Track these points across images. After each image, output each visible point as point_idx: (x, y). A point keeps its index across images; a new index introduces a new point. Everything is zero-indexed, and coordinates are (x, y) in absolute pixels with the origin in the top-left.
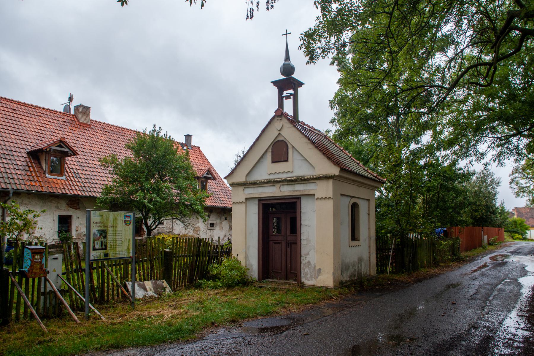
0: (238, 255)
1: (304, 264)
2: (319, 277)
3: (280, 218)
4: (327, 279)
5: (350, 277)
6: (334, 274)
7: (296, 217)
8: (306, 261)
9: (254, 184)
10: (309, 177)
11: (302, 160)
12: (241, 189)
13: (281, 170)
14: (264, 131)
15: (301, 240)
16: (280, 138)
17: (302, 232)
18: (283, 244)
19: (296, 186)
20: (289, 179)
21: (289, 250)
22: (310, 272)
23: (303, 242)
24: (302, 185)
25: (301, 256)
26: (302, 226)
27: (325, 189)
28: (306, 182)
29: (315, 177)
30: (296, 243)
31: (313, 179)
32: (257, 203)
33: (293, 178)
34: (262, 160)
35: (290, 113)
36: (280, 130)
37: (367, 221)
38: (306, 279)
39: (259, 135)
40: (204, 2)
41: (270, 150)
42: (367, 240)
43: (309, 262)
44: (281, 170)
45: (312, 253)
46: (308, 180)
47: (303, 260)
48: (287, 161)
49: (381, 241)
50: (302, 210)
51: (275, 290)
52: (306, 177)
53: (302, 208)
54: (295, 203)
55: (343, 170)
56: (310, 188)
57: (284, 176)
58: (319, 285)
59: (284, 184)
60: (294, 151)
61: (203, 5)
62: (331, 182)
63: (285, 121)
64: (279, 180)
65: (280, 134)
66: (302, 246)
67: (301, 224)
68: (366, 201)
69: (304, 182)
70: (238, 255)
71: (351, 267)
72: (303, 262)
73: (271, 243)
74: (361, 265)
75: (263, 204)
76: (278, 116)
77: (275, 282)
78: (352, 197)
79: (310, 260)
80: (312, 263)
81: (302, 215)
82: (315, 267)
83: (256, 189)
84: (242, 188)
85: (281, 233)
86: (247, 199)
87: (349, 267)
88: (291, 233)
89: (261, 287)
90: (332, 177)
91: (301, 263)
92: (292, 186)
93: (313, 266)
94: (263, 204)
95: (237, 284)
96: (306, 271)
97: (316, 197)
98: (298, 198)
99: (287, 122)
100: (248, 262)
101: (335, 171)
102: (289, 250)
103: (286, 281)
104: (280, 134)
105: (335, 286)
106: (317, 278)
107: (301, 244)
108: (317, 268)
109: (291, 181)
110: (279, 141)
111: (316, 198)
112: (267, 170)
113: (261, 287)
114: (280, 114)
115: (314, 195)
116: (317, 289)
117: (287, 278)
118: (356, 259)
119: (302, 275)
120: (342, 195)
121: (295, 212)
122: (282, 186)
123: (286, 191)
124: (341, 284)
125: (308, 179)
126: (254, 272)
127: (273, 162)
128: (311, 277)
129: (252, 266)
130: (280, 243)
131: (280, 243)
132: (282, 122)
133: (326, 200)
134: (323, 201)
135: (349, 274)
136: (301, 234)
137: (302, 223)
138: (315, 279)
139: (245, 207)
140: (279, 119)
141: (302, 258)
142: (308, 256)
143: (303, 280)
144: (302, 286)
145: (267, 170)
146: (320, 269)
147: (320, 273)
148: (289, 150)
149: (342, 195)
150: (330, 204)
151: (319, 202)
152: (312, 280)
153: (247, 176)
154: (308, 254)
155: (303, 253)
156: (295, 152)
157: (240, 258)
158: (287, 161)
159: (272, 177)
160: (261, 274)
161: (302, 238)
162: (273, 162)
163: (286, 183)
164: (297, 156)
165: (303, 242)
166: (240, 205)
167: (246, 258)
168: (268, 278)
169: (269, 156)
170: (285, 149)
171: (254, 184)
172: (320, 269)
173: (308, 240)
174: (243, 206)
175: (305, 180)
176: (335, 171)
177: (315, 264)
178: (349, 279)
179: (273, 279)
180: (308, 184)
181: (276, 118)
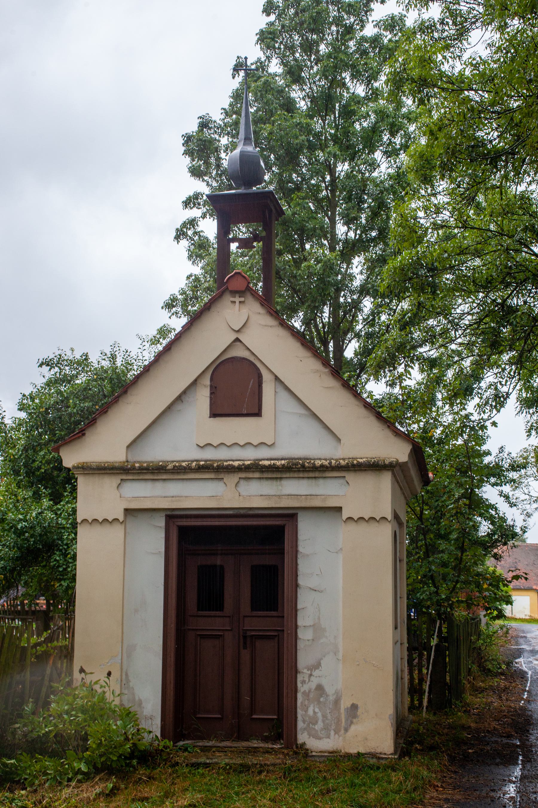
0: (109, 674)
1: (306, 694)
2: (353, 728)
4: (374, 732)
8: (313, 685)
9: (157, 471)
10: (326, 463)
11: (301, 415)
12: (109, 483)
13: (238, 439)
15: (296, 627)
16: (239, 352)
17: (299, 606)
19: (284, 482)
20: (267, 463)
21: (246, 655)
22: (324, 716)
23: (304, 635)
24: (305, 482)
25: (296, 672)
28: (317, 474)
29: (343, 463)
31: (339, 468)
33: (278, 463)
34: (179, 407)
36: (238, 331)
38: (310, 735)
41: (207, 381)
43: (320, 688)
44: (238, 439)
45: (327, 663)
46: (323, 469)
47: (303, 682)
48: (258, 414)
50: (300, 549)
52: (318, 463)
56: (328, 491)
57: (249, 455)
58: (353, 751)
59: (251, 475)
60: (280, 389)
64: (236, 464)
65: (237, 340)
66: (301, 645)
67: (297, 586)
69: (311, 475)
70: (109, 674)
72: (302, 688)
79: (324, 682)
80: (330, 690)
81: (300, 561)
82: (337, 702)
83: (159, 485)
84: (114, 481)
86: (127, 511)
88: (253, 609)
92: (274, 483)
93: (332, 698)
96: (310, 712)
97: (345, 516)
102: (246, 655)
103: (245, 744)
104: (237, 340)
106: (346, 730)
108: (345, 704)
109: (272, 469)
110: (233, 359)
111: (344, 517)
113: (196, 766)
119: (300, 725)
121: (281, 552)
122: (242, 482)
123: (256, 495)
125: (322, 466)
127: (214, 414)
128: (326, 728)
129: (140, 703)
131: (217, 637)
133: (374, 525)
134: (363, 526)
137: (301, 581)
138: (337, 732)
140: (237, 299)
141: (300, 678)
142: (316, 673)
143: (302, 737)
144: (302, 752)
146: (354, 707)
147: (355, 716)
148: (264, 385)
151: (352, 526)
152: (328, 737)
153: (128, 447)
154: (318, 666)
155: (304, 660)
156: (283, 395)
158: (258, 414)
159: (209, 455)
161: (300, 623)
162: (214, 414)
163: (257, 475)
164: (286, 404)
165: (300, 634)
166: (106, 530)
169: (202, 398)
171: (157, 471)
173: (317, 628)
174: (118, 531)
175: (315, 469)
180: (321, 481)
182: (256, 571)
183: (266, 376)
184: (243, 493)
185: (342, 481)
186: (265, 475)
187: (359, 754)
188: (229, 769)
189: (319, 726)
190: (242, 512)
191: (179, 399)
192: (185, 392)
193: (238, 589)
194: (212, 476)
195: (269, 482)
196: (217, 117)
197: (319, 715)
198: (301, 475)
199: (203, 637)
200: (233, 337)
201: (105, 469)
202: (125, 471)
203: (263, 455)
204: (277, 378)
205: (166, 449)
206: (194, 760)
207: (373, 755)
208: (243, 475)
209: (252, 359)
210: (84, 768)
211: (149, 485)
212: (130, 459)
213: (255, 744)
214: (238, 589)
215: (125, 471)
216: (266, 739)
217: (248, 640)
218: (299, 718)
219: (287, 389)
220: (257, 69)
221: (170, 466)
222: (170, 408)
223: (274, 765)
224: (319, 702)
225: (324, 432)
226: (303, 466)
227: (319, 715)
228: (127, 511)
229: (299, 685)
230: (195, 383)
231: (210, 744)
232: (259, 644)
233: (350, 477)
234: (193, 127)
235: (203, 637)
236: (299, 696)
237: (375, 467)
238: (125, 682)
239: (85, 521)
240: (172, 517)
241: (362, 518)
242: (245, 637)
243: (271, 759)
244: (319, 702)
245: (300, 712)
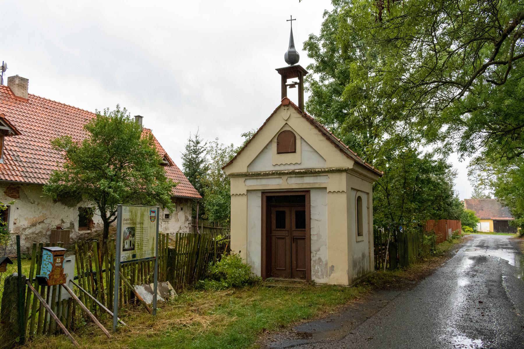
0: (240, 252)
1: (315, 261)
2: (332, 274)
3: (287, 212)
4: (341, 277)
5: (357, 274)
6: (348, 271)
7: (305, 211)
9: (258, 175)
10: (320, 170)
11: (311, 152)
12: (242, 180)
13: (287, 162)
14: (268, 120)
15: (310, 235)
17: (311, 227)
18: (288, 240)
19: (305, 178)
20: (297, 171)
21: (294, 245)
23: (313, 238)
25: (311, 253)
27: (339, 183)
28: (317, 175)
29: (326, 170)
31: (325, 172)
33: (302, 171)
34: (266, 150)
36: (286, 120)
38: (316, 277)
41: (276, 140)
43: (320, 259)
44: (287, 162)
45: (323, 249)
46: (319, 172)
47: (313, 256)
48: (295, 152)
49: (377, 236)
50: (311, 204)
51: (287, 289)
52: (317, 170)
53: (311, 202)
54: (304, 196)
55: (357, 163)
56: (321, 181)
57: (291, 168)
58: (333, 284)
59: (292, 176)
60: (303, 142)
62: (344, 175)
63: (292, 111)
64: (286, 172)
65: (286, 124)
66: (312, 242)
67: (310, 219)
69: (315, 175)
70: (240, 252)
72: (313, 259)
73: (274, 238)
75: (267, 197)
76: (285, 106)
78: (358, 190)
80: (324, 260)
82: (326, 264)
83: (259, 180)
84: (243, 179)
85: (284, 228)
86: (248, 191)
88: (297, 228)
89: (270, 287)
90: (346, 171)
91: (311, 260)
94: (267, 197)
95: (243, 283)
96: (316, 268)
97: (328, 190)
98: (307, 191)
100: (249, 259)
101: (349, 164)
102: (294, 245)
103: (292, 280)
105: (350, 285)
106: (330, 276)
108: (330, 265)
110: (285, 131)
111: (328, 191)
112: (271, 161)
113: (270, 287)
114: (286, 103)
115: (326, 188)
116: (335, 288)
117: (292, 277)
118: (361, 256)
119: (312, 273)
120: (352, 189)
121: (304, 206)
124: (355, 283)
125: (318, 171)
127: (278, 153)
128: (322, 275)
129: (254, 263)
130: (283, 238)
131: (283, 238)
132: (289, 113)
134: (335, 195)
136: (310, 229)
137: (312, 217)
139: (246, 199)
140: (286, 108)
141: (312, 255)
142: (318, 253)
143: (313, 278)
144: (313, 284)
145: (271, 161)
146: (333, 266)
147: (333, 270)
148: (297, 141)
149: (352, 189)
150: (343, 198)
151: (331, 195)
152: (323, 278)
153: (248, 166)
154: (319, 250)
155: (313, 248)
156: (304, 143)
157: (242, 256)
158: (295, 152)
159: (277, 168)
161: (312, 233)
162: (278, 153)
163: (294, 176)
164: (305, 147)
165: (312, 238)
166: (241, 197)
167: (248, 255)
168: (271, 276)
169: (274, 147)
170: (292, 140)
171: (258, 175)
172: (333, 266)
173: (318, 235)
174: (244, 199)
175: (316, 172)
176: (349, 164)
177: (327, 262)
179: (278, 277)
180: (319, 177)
181: (283, 108)
182: (297, 213)
183: (298, 137)
184: (289, 183)
185: (326, 177)
186: (297, 176)
187: (335, 285)
188: (281, 289)
189: (320, 273)
190: (289, 190)
191: (266, 147)
192: (268, 145)
193: (290, 220)
194: (278, 176)
195: (299, 178)
196: (318, 34)
197: (320, 269)
198: (311, 175)
199: (278, 238)
200: (285, 122)
201: (239, 175)
202: (246, 176)
203: (297, 168)
204: (301, 138)
205: (260, 167)
206: (270, 285)
207: (340, 286)
208: (289, 176)
209: (292, 131)
210: (226, 285)
211: (255, 180)
212: (249, 171)
213: (281, 279)
214: (290, 220)
215: (246, 176)
216: (302, 278)
217: (295, 240)
218: (312, 270)
219: (305, 141)
220: (334, 13)
221: (262, 173)
222: (262, 151)
223: (298, 288)
224: (320, 264)
225: (320, 158)
226: (311, 172)
227: (320, 269)
228: (248, 191)
229: (312, 257)
230: (271, 141)
231: (295, 280)
232: (299, 241)
233: (330, 175)
235: (278, 238)
236: (312, 262)
237: (339, 171)
238: (248, 255)
239: (233, 195)
240: (264, 192)
242: (294, 239)
243: (299, 286)
244: (320, 264)
245: (312, 268)
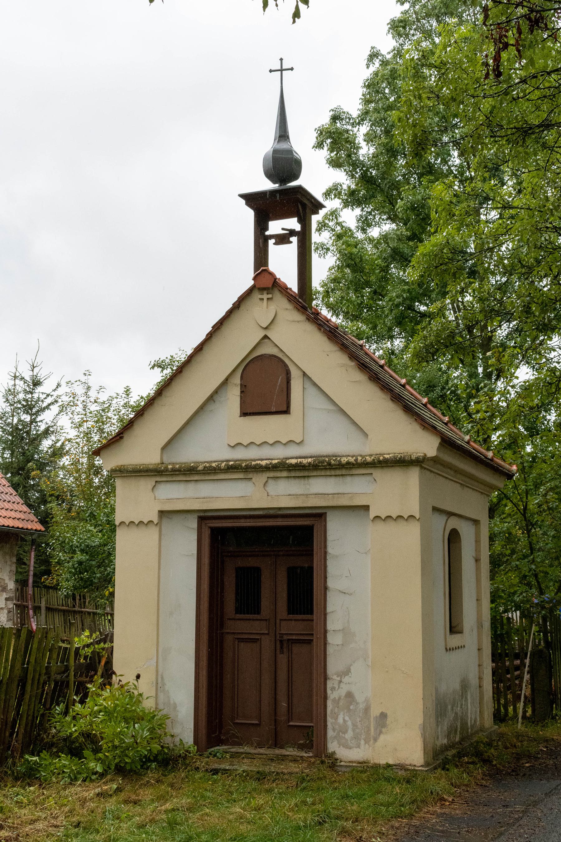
0: (138, 677)
1: (336, 702)
2: (382, 737)
3: (263, 570)
4: (404, 743)
5: (448, 736)
6: (424, 728)
7: (311, 569)
8: (342, 692)
9: (189, 472)
10: (352, 460)
11: (329, 411)
12: (146, 484)
13: (268, 437)
14: (218, 326)
15: (326, 631)
16: (267, 350)
17: (329, 610)
18: (267, 643)
19: (312, 481)
20: (293, 461)
21: (283, 659)
22: (354, 725)
23: (334, 639)
24: (332, 480)
25: (326, 678)
26: (329, 594)
27: (401, 493)
28: (344, 472)
29: (369, 459)
30: (310, 642)
31: (365, 465)
32: (195, 525)
33: (305, 461)
35: (291, 281)
36: (266, 328)
37: (474, 580)
38: (340, 744)
39: (203, 337)
40: (300, 4)
41: (237, 380)
42: (475, 631)
43: (349, 695)
44: (268, 437)
45: (358, 669)
46: (349, 466)
47: (333, 689)
48: (287, 411)
49: (500, 632)
50: (330, 550)
51: (261, 777)
52: (344, 460)
53: (330, 544)
54: (309, 529)
55: (447, 443)
56: (355, 488)
57: (277, 454)
58: (383, 762)
59: (278, 474)
60: (308, 385)
61: (297, 14)
62: (414, 476)
63: (281, 304)
64: (264, 463)
65: (266, 337)
66: (330, 650)
67: (326, 588)
68: (470, 524)
69: (338, 472)
70: (138, 677)
71: (449, 707)
72: (332, 695)
73: (229, 639)
74: (466, 700)
75: (213, 530)
76: (262, 290)
77: (248, 755)
78: (450, 514)
79: (353, 689)
80: (360, 698)
81: (329, 563)
82: (367, 710)
83: (191, 486)
84: (150, 482)
85: (259, 613)
86: (162, 513)
87: (446, 706)
89: (215, 772)
90: (418, 462)
91: (325, 698)
92: (302, 481)
93: (362, 706)
94: (213, 530)
95: (146, 761)
96: (340, 720)
97: (373, 513)
98: (319, 516)
99: (288, 306)
100: (161, 696)
101: (428, 446)
102: (283, 659)
103: (278, 751)
104: (266, 337)
105: (427, 764)
106: (375, 740)
107: (325, 644)
108: (375, 712)
109: (299, 467)
111: (372, 515)
112: (226, 434)
113: (215, 772)
114: (265, 283)
115: (366, 508)
116: (387, 774)
117: (277, 743)
118: (457, 686)
119: (330, 733)
120: (435, 509)
121: (310, 554)
122: (270, 481)
123: (284, 495)
124: (441, 758)
125: (348, 463)
126: (183, 726)
127: (244, 414)
128: (356, 737)
130: (255, 641)
131: (255, 641)
132: (273, 308)
133: (402, 523)
134: (391, 527)
135: (445, 728)
136: (325, 615)
138: (367, 742)
139: (156, 537)
140: (265, 296)
141: (329, 684)
142: (346, 679)
143: (333, 746)
144: (333, 763)
145: (226, 434)
146: (383, 716)
147: (384, 725)
148: (293, 382)
149: (435, 509)
150: (411, 535)
151: (380, 527)
152: (358, 746)
153: (163, 449)
154: (347, 672)
155: (334, 666)
156: (311, 390)
157: (145, 687)
158: (287, 411)
159: (241, 454)
160: (203, 731)
161: (330, 627)
163: (285, 474)
164: (315, 401)
165: (331, 638)
167: (159, 685)
168: (220, 742)
169: (233, 396)
170: (281, 380)
171: (189, 472)
172: (383, 716)
173: (346, 632)
174: (152, 534)
175: (341, 466)
176: (428, 446)
177: (367, 701)
178: (445, 741)
179: (239, 744)
180: (349, 479)
181: (257, 296)
182: (291, 572)
183: (295, 373)
184: (271, 493)
185: (368, 478)
186: (293, 474)
187: (388, 766)
188: (246, 776)
189: (349, 735)
190: (272, 512)
191: (211, 398)
192: (216, 392)
193: (274, 590)
194: (241, 476)
195: (297, 481)
196: (354, 108)
197: (349, 723)
198: (328, 473)
199: (241, 640)
200: (261, 334)
201: (140, 471)
202: (159, 473)
203: (291, 454)
204: (304, 374)
206: (216, 766)
207: (402, 767)
208: (272, 474)
209: (280, 355)
211: (182, 486)
212: (165, 460)
214: (274, 590)
215: (159, 473)
216: (302, 747)
217: (284, 644)
219: (315, 384)
221: (201, 468)
222: (202, 408)
223: (291, 774)
224: (349, 710)
225: (352, 428)
226: (329, 464)
227: (349, 723)
228: (162, 513)
229: (329, 692)
230: (226, 382)
231: (284, 752)
232: (296, 649)
233: (377, 473)
234: (325, 120)
235: (241, 640)
236: (329, 704)
237: (401, 463)
238: (159, 685)
239: (122, 523)
240: (204, 518)
241: (400, 517)
242: (281, 642)
243: (294, 768)
244: (349, 710)
245: (330, 720)
